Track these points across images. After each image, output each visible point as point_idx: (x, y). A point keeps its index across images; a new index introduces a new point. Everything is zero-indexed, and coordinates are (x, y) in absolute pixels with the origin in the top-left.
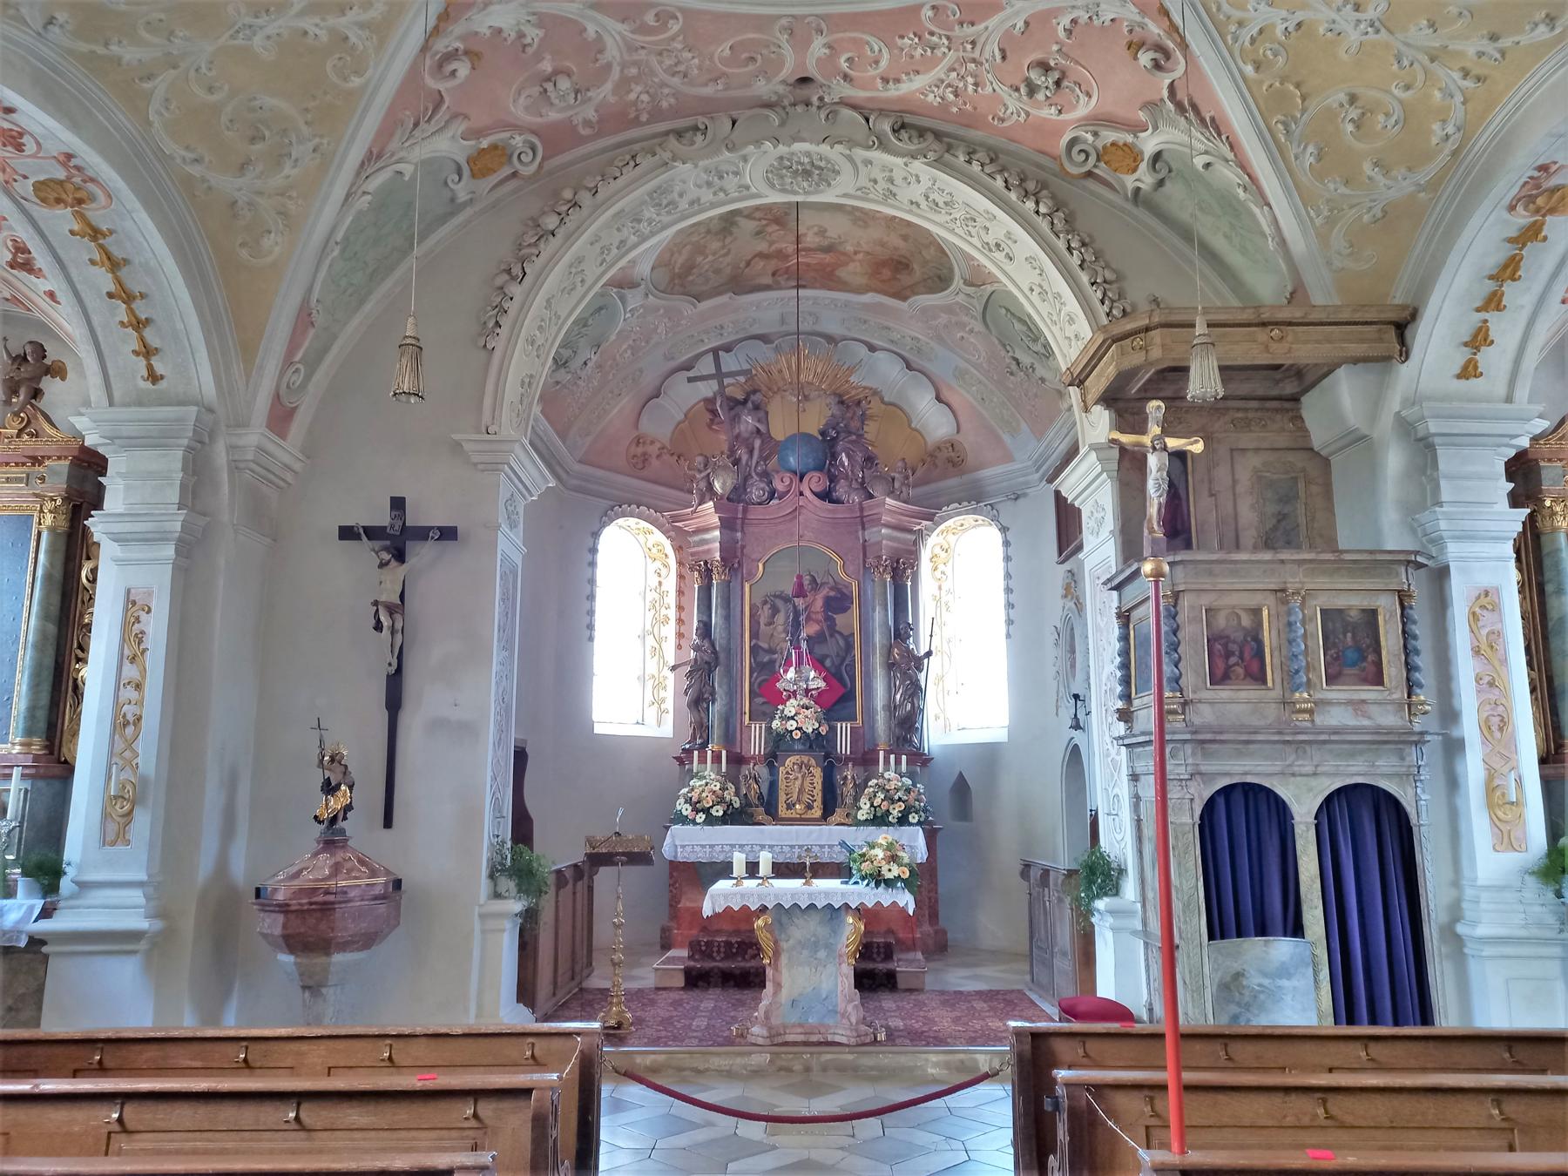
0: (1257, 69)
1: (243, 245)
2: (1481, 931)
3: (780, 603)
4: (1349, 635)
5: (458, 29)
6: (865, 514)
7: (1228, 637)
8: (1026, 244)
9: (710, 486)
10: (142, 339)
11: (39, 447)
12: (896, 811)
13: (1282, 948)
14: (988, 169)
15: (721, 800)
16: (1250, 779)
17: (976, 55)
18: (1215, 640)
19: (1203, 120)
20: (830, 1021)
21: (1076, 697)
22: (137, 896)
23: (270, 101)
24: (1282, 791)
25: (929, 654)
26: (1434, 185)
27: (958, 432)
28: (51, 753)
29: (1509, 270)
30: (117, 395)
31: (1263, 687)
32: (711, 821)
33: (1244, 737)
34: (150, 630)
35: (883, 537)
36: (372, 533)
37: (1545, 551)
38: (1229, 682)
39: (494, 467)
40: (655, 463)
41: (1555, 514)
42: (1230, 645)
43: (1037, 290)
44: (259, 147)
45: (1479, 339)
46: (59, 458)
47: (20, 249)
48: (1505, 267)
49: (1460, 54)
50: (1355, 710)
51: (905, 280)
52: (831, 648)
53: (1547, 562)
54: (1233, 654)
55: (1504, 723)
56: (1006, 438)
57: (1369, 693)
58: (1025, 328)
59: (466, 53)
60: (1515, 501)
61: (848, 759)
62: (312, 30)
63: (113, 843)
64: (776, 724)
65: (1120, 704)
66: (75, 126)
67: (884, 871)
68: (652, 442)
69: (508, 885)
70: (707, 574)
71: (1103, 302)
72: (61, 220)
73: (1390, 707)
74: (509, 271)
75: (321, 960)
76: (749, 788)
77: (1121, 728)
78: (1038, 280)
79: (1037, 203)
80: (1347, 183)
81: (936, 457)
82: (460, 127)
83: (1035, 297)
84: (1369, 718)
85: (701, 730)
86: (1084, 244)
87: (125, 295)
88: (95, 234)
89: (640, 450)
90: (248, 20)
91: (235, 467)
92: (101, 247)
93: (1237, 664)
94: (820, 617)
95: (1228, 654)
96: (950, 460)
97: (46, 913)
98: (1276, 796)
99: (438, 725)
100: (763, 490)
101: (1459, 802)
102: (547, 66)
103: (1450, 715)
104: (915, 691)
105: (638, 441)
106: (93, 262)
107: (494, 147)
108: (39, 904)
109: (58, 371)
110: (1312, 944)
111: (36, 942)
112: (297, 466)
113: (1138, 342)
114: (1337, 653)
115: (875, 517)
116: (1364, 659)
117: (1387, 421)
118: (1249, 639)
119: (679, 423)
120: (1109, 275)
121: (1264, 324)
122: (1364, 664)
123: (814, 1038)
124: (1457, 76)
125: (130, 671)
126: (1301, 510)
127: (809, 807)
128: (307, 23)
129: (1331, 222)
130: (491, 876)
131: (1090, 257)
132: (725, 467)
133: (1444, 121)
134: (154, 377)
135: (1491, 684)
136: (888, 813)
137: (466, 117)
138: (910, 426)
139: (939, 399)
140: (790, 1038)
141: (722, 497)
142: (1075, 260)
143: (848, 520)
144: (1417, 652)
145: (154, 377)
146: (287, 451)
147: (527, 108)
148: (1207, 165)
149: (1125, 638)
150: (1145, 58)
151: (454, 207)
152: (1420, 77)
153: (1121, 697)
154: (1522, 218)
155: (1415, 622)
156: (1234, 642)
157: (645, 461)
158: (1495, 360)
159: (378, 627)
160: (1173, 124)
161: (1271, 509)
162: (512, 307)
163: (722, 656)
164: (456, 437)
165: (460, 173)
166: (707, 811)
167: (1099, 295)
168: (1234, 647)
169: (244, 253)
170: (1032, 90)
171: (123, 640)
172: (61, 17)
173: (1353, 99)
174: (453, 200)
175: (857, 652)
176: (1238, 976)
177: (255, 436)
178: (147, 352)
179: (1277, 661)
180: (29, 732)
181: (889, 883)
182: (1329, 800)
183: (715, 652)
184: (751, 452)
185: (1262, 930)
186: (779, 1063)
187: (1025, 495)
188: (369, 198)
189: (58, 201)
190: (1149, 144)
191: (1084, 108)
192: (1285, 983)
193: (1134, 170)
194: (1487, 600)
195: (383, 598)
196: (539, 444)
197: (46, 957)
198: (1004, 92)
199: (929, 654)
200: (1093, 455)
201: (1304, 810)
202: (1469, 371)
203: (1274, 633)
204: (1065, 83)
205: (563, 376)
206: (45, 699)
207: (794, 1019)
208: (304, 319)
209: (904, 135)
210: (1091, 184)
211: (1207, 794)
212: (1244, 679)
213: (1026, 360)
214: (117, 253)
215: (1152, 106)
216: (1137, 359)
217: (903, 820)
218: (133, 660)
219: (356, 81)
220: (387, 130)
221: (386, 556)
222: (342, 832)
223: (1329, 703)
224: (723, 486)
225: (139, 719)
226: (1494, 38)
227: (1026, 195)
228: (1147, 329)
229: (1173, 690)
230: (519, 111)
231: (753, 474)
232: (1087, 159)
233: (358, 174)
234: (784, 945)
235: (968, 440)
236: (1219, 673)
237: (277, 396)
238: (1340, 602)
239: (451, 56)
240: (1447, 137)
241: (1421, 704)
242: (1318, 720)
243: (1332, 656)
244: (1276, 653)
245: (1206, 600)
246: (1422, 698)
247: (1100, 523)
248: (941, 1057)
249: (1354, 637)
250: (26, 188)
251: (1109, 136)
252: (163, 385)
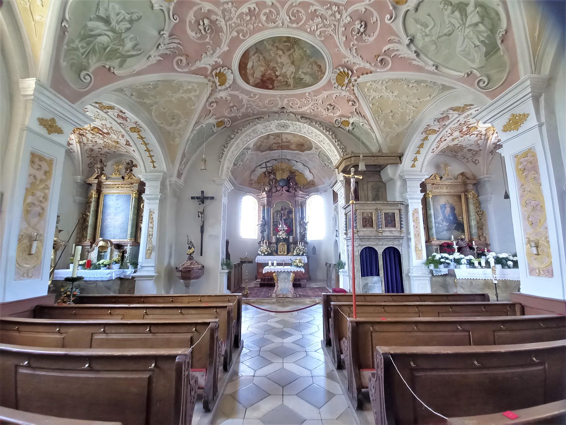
0: (372, 106)
1: (171, 140)
2: (414, 275)
3: (278, 212)
5: (214, 97)
8: (327, 141)
9: (265, 189)
10: (152, 159)
11: (132, 181)
12: (301, 253)
13: (375, 278)
14: (320, 126)
15: (267, 251)
16: (370, 246)
17: (317, 102)
19: (362, 116)
20: (288, 293)
21: (337, 231)
22: (153, 269)
23: (176, 111)
24: (376, 248)
25: (308, 222)
26: (407, 129)
28: (136, 241)
29: (421, 146)
30: (147, 171)
32: (265, 255)
33: (369, 238)
34: (154, 217)
35: (299, 199)
36: (198, 198)
37: (427, 201)
39: (221, 185)
41: (429, 194)
43: (329, 150)
44: (174, 121)
45: (415, 160)
46: (136, 183)
47: (127, 141)
48: (421, 145)
49: (412, 102)
51: (303, 148)
52: (288, 221)
53: (427, 204)
54: (367, 222)
55: (419, 235)
56: (323, 180)
57: (393, 229)
59: (215, 102)
60: (422, 191)
61: (292, 243)
62: (184, 97)
63: (148, 259)
64: (278, 236)
65: (345, 232)
66: (137, 116)
67: (299, 264)
69: (225, 267)
70: (264, 207)
71: (342, 152)
72: (135, 135)
74: (224, 146)
75: (188, 281)
76: (272, 249)
77: (345, 236)
78: (329, 148)
79: (329, 132)
80: (390, 128)
82: (214, 117)
83: (329, 151)
85: (263, 237)
86: (338, 141)
87: (148, 151)
88: (142, 138)
89: (251, 182)
90: (171, 95)
91: (170, 185)
92: (143, 141)
94: (286, 215)
95: (366, 222)
96: (312, 184)
97: (135, 272)
98: (375, 249)
99: (211, 236)
101: (410, 250)
102: (232, 105)
103: (408, 233)
104: (305, 229)
105: (250, 180)
106: (142, 144)
107: (221, 121)
108: (133, 270)
109: (136, 166)
110: (381, 277)
111: (133, 278)
112: (183, 185)
113: (349, 160)
117: (397, 176)
120: (344, 147)
121: (373, 156)
123: (285, 296)
124: (412, 107)
125: (151, 225)
126: (380, 193)
127: (284, 252)
128: (183, 95)
129: (387, 136)
130: (222, 265)
131: (339, 143)
132: (268, 185)
133: (409, 116)
134: (154, 167)
135: (416, 227)
136: (300, 253)
137: (216, 115)
140: (280, 296)
142: (337, 144)
144: (402, 221)
145: (154, 167)
146: (181, 182)
147: (228, 113)
148: (363, 125)
149: (346, 219)
150: (350, 103)
151: (214, 133)
152: (405, 107)
153: (345, 230)
154: (424, 135)
158: (418, 164)
159: (199, 216)
160: (356, 117)
161: (375, 193)
162: (225, 153)
163: (267, 223)
164: (214, 179)
165: (214, 126)
166: (264, 253)
167: (341, 151)
168: (367, 220)
169: (172, 142)
170: (328, 110)
171: (149, 219)
172: (134, 94)
173: (391, 111)
174: (213, 132)
175: (294, 222)
176: (367, 284)
177: (174, 178)
178: (153, 162)
179: (375, 223)
180: (131, 237)
181: (300, 267)
182: (385, 250)
183: (265, 222)
185: (372, 275)
186: (278, 301)
188: (196, 131)
189: (135, 131)
190: (351, 121)
191: (338, 113)
192: (376, 285)
193: (348, 126)
194: (416, 211)
195: (199, 211)
196: (230, 180)
197: (135, 280)
198: (322, 110)
199: (308, 222)
200: (340, 182)
201: (380, 251)
202: (413, 166)
203: (375, 218)
204: (335, 108)
205: (236, 167)
206: (134, 230)
207: (281, 293)
208: (184, 155)
209: (303, 119)
210: (340, 129)
211: (361, 249)
213: (327, 164)
214: (146, 142)
215: (352, 113)
216: (349, 163)
217: (303, 255)
218: (151, 223)
219: (193, 107)
220: (199, 118)
221: (200, 202)
222: (192, 256)
223: (385, 231)
224: (267, 189)
225: (153, 234)
226: (419, 99)
227: (327, 131)
228: (351, 157)
229: (355, 229)
230: (226, 114)
232: (339, 123)
233: (194, 126)
234: (279, 279)
235: (316, 180)
236: (364, 225)
237: (179, 171)
238: (388, 211)
239: (212, 102)
240: (410, 119)
242: (383, 234)
245: (362, 211)
247: (341, 196)
248: (310, 300)
250: (128, 129)
251: (344, 119)
252: (156, 168)
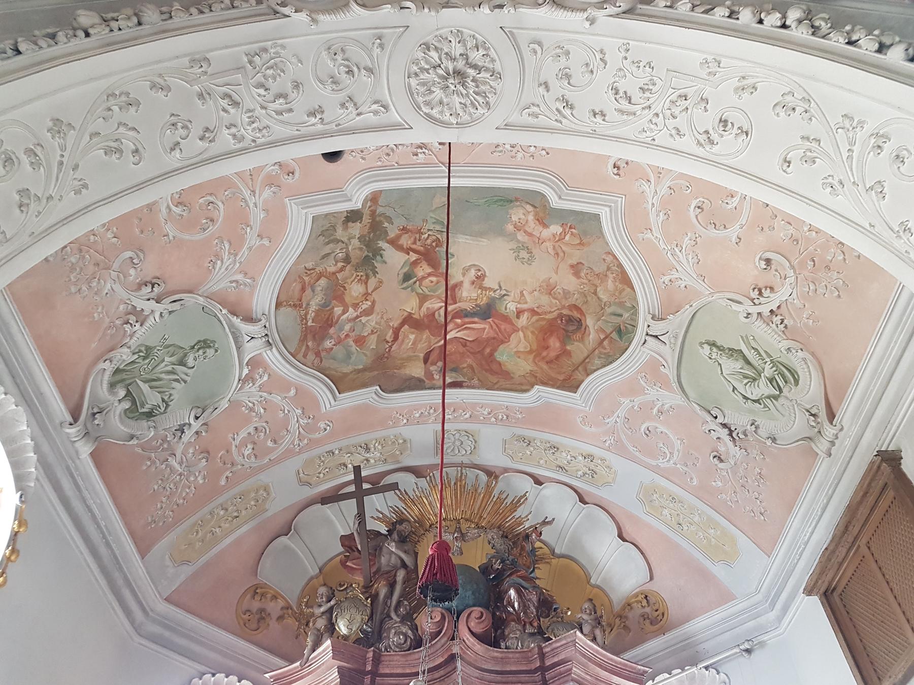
6: (548, 663)
27: (651, 578)
40: (273, 624)
51: (579, 350)
56: (718, 571)
58: (738, 365)
68: (275, 597)
81: (626, 617)
89: (256, 605)
96: (644, 617)
100: (405, 635)
115: (562, 668)
119: (312, 579)
138: (588, 582)
139: (621, 536)
141: (345, 638)
143: (523, 677)
157: (261, 619)
184: (392, 586)
187: (762, 644)
231: (393, 615)
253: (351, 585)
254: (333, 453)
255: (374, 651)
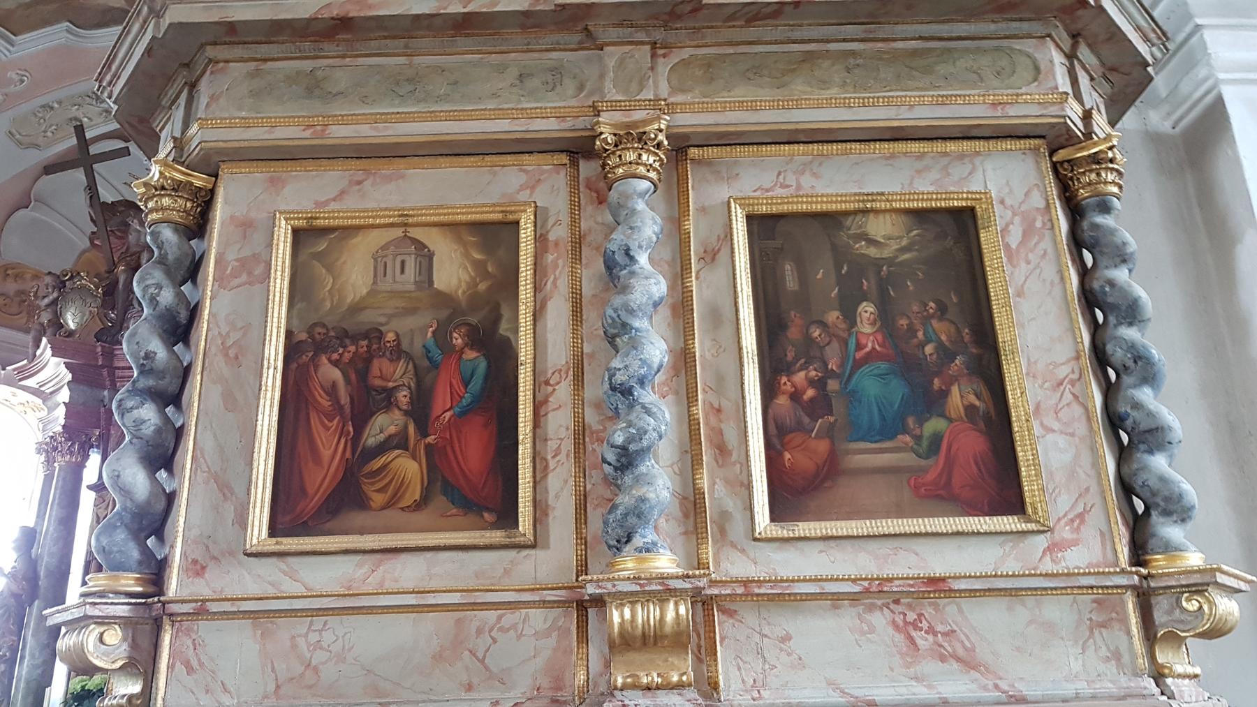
4: (867, 310)
7: (374, 334)
18: (321, 347)
31: (497, 536)
38: (359, 518)
42: (380, 366)
50: (905, 628)
54: (387, 400)
73: (1057, 611)
84: (969, 663)
93: (399, 442)
114: (820, 384)
116: (933, 403)
118: (458, 341)
119: (84, 252)
122: (934, 425)
141: (70, 334)
155: (1123, 258)
156: (398, 352)
168: (397, 374)
212: (418, 506)
241: (1198, 589)
243: (795, 396)
244: (563, 392)
246: (1194, 559)
249: (885, 317)
253: (79, 273)
254: (52, 108)
255: (101, 345)
